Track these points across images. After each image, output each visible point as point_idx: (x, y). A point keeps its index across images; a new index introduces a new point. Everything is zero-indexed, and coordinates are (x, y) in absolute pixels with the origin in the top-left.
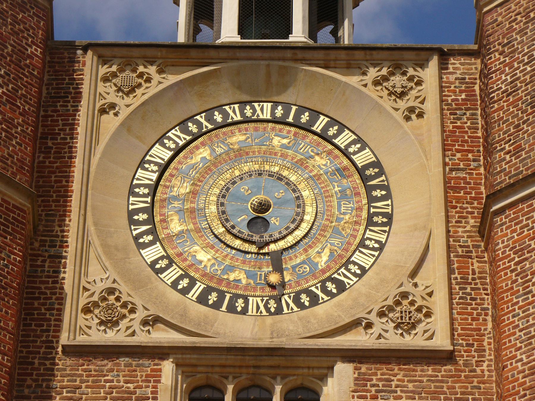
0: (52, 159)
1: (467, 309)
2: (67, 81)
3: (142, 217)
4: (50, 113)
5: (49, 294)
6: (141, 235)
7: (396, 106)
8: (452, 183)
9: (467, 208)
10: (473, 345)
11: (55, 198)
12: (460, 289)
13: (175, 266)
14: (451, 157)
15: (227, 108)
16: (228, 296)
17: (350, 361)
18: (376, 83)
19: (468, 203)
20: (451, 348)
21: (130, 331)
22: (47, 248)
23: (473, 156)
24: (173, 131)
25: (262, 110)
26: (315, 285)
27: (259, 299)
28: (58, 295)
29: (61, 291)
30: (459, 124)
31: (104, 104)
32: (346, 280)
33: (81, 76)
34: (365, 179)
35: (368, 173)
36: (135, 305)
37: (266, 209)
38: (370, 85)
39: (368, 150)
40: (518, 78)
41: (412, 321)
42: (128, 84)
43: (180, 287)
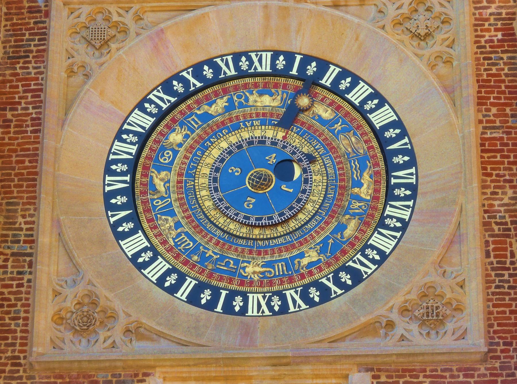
0: (12, 135)
1: (504, 299)
2: (27, 36)
3: (120, 200)
4: (8, 78)
5: (13, 300)
6: (119, 223)
7: (420, 52)
8: (487, 145)
9: (504, 175)
10: (511, 344)
11: (16, 182)
12: (497, 275)
13: (160, 259)
14: (484, 113)
16: (224, 293)
17: (367, 370)
19: (505, 169)
21: (110, 341)
22: (9, 244)
23: (511, 110)
24: (155, 92)
25: (260, 61)
26: (326, 276)
27: (260, 296)
28: (23, 301)
29: (27, 296)
30: (494, 71)
31: (72, 65)
32: (362, 269)
33: (44, 30)
34: (383, 142)
35: (387, 134)
36: (114, 310)
37: (267, 184)
39: (387, 107)
41: (441, 318)
42: (99, 38)
43: (167, 284)
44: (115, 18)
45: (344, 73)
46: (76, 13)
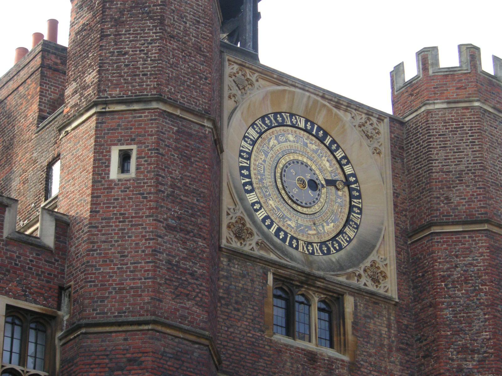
3: (245, 172)
13: (263, 210)
15: (283, 114)
18: (360, 126)
20: (397, 300)
21: (251, 247)
25: (300, 121)
31: (231, 94)
32: (342, 243)
38: (357, 126)
40: (449, 159)
44: (248, 77)
45: (333, 142)
46: (232, 67)
